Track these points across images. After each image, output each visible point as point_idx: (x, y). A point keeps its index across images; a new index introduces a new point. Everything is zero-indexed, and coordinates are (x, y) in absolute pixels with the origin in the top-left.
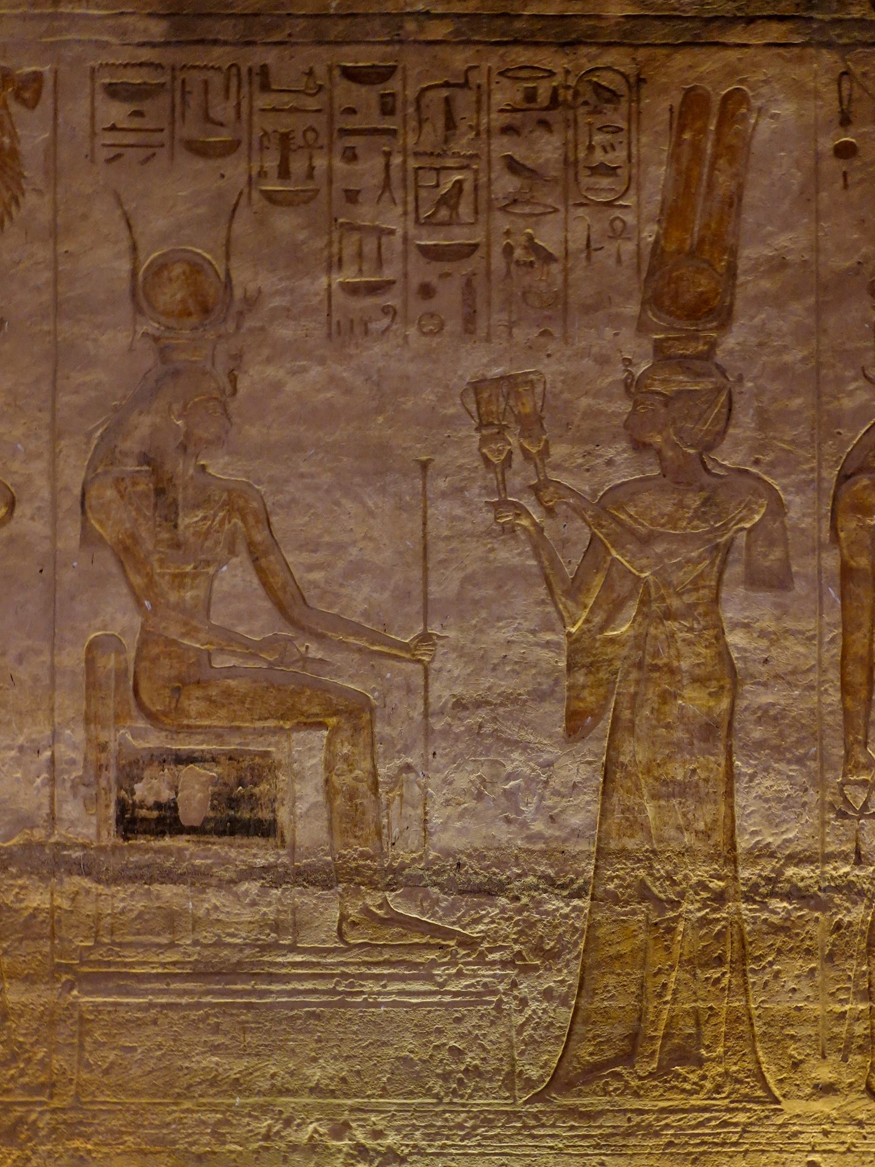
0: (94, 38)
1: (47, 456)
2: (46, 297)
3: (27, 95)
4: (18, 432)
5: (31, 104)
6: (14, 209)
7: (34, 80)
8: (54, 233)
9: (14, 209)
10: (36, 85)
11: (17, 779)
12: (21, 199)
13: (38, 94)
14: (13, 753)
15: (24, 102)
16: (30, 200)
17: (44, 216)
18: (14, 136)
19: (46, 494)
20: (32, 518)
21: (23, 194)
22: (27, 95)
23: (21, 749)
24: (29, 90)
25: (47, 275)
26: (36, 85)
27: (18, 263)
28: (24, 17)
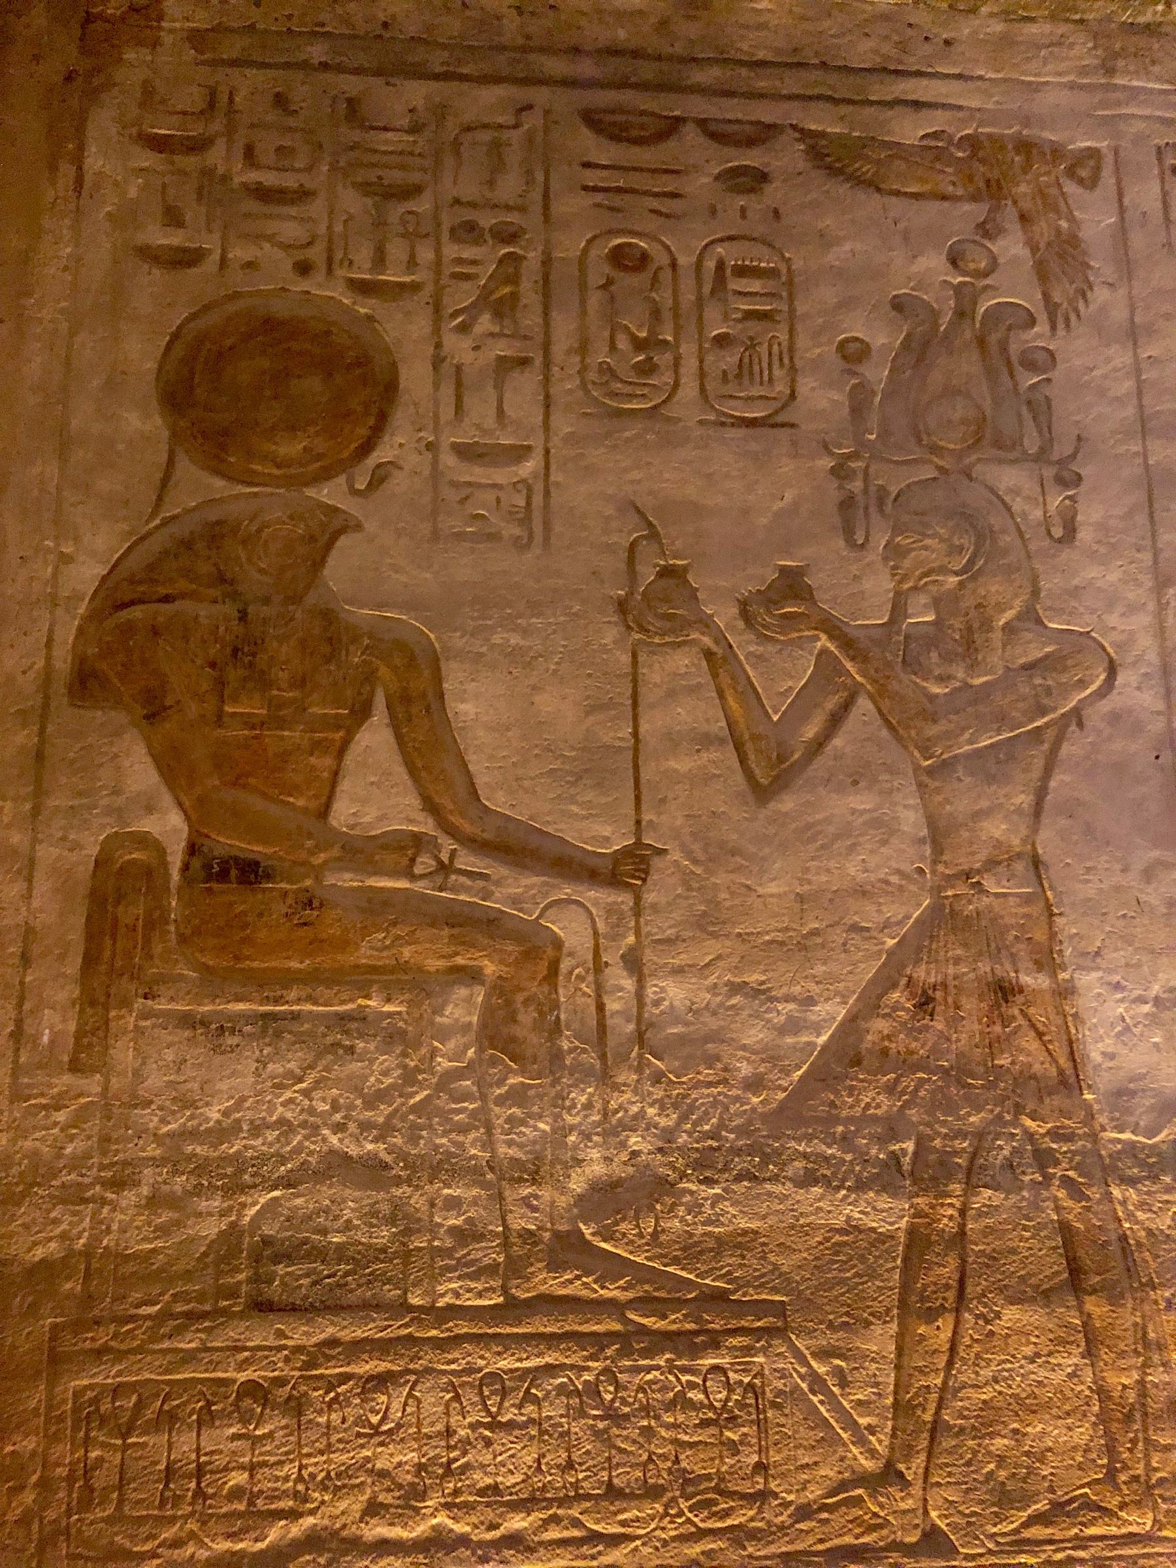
0: (1159, 113)
1: (1151, 606)
2: (1130, 411)
3: (1083, 173)
4: (1113, 577)
5: (1092, 183)
6: (1081, 305)
7: (1091, 157)
8: (1133, 334)
9: (1081, 305)
10: (1092, 163)
11: (1156, 1045)
12: (1089, 294)
13: (1098, 169)
14: (1146, 1008)
15: (1081, 182)
16: (1100, 295)
17: (1119, 314)
18: (1071, 219)
19: (1153, 657)
20: (1139, 688)
21: (1091, 288)
22: (1083, 173)
23: (1157, 1001)
24: (1085, 168)
25: (1128, 385)
26: (1092, 163)
27: (1092, 370)
28: (1072, 86)
